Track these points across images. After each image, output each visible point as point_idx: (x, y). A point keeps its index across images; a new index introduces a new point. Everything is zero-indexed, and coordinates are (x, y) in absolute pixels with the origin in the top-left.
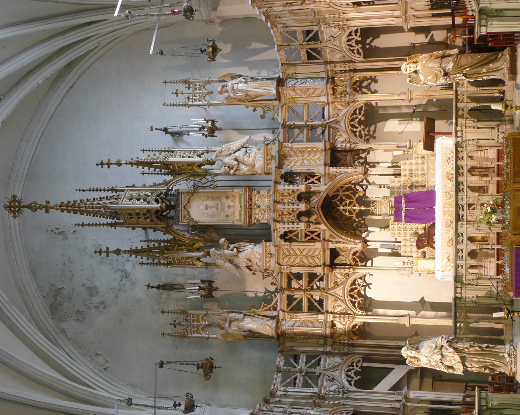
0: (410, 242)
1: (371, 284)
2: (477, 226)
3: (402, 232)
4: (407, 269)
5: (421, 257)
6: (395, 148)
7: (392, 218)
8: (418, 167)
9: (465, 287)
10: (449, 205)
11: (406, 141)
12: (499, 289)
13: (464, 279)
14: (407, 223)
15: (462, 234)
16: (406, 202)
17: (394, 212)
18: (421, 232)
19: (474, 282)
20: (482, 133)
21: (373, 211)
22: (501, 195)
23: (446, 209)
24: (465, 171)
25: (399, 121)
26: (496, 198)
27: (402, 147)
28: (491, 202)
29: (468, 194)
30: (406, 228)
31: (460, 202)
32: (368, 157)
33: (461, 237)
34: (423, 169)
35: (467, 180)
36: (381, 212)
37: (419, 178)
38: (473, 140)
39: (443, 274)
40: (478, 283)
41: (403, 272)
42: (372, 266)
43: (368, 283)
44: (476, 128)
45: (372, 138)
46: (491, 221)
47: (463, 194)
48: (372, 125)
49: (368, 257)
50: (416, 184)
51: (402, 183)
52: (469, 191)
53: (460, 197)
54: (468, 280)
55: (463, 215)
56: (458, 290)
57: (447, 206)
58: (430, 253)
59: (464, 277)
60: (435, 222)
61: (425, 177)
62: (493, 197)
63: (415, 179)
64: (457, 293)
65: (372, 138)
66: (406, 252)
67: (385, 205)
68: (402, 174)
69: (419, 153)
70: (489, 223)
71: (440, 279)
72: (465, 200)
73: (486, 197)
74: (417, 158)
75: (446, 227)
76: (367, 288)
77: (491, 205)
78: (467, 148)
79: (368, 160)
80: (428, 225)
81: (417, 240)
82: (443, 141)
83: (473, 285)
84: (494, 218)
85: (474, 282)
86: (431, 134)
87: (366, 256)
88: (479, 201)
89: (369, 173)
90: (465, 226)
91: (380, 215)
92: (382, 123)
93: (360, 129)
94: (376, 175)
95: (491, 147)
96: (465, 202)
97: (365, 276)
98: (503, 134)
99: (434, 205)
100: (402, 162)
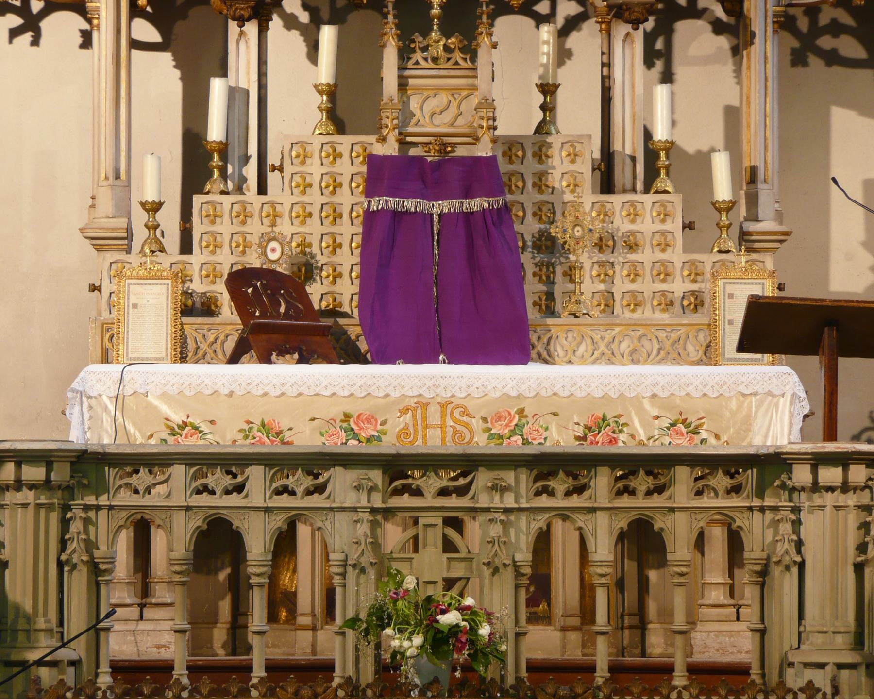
0: (266, 239)
1: (35, 42)
2: (365, 561)
3: (315, 198)
4: (122, 222)
6: (746, 164)
7: (390, 149)
8: (648, 278)
9: (49, 507)
10: (456, 432)
11: (779, 217)
12: (44, 672)
13: (90, 500)
14: (358, 222)
15: (320, 489)
16: (468, 216)
17: (420, 160)
18: (315, 291)
19: (76, 551)
20: (834, 586)
21: (425, 49)
22: (518, 679)
23: (434, 417)
24: (639, 502)
26: (504, 654)
27: (753, 200)
28: (484, 631)
29: (523, 521)
31: (483, 478)
32: (701, 26)
33: (308, 482)
34: (635, 302)
35: (593, 510)
36: (419, 89)
38: (799, 544)
39: (105, 399)
40: (74, 567)
41: (106, 205)
42: (136, 45)
43: (44, 24)
44: (859, 559)
45: (796, 44)
46: (389, 631)
47: (523, 490)
48: (868, 49)
49: (179, 27)
50: (559, 270)
51: (568, 197)
52: (540, 521)
53: (509, 477)
54: (87, 521)
55: (418, 492)
56: (34, 473)
57: (450, 423)
58: (211, 338)
59: (103, 500)
60: (365, 361)
61: (595, 312)
62: (511, 636)
63: (587, 266)
64: (18, 465)
65: (796, 44)
66: (214, 218)
67: (453, 109)
68: (616, 200)
69: (720, 283)
70: (380, 619)
71: (74, 385)
72: (497, 503)
73: (509, 603)
74: (696, 275)
75: (347, 416)
76: (15, 21)
77: (474, 630)
78: (757, 515)
79: (683, 28)
80: (354, 331)
81: (273, 272)
82: (784, 403)
83: (63, 544)
84: (406, 644)
85: (76, 551)
86: (829, 336)
87: (184, 17)
88: (487, 572)
89: (621, 29)
90: (364, 503)
91: (403, 86)
94: (607, 65)
95: (763, 632)
96: (484, 501)
98: (829, 690)
99: (453, 359)
100: (676, 200)
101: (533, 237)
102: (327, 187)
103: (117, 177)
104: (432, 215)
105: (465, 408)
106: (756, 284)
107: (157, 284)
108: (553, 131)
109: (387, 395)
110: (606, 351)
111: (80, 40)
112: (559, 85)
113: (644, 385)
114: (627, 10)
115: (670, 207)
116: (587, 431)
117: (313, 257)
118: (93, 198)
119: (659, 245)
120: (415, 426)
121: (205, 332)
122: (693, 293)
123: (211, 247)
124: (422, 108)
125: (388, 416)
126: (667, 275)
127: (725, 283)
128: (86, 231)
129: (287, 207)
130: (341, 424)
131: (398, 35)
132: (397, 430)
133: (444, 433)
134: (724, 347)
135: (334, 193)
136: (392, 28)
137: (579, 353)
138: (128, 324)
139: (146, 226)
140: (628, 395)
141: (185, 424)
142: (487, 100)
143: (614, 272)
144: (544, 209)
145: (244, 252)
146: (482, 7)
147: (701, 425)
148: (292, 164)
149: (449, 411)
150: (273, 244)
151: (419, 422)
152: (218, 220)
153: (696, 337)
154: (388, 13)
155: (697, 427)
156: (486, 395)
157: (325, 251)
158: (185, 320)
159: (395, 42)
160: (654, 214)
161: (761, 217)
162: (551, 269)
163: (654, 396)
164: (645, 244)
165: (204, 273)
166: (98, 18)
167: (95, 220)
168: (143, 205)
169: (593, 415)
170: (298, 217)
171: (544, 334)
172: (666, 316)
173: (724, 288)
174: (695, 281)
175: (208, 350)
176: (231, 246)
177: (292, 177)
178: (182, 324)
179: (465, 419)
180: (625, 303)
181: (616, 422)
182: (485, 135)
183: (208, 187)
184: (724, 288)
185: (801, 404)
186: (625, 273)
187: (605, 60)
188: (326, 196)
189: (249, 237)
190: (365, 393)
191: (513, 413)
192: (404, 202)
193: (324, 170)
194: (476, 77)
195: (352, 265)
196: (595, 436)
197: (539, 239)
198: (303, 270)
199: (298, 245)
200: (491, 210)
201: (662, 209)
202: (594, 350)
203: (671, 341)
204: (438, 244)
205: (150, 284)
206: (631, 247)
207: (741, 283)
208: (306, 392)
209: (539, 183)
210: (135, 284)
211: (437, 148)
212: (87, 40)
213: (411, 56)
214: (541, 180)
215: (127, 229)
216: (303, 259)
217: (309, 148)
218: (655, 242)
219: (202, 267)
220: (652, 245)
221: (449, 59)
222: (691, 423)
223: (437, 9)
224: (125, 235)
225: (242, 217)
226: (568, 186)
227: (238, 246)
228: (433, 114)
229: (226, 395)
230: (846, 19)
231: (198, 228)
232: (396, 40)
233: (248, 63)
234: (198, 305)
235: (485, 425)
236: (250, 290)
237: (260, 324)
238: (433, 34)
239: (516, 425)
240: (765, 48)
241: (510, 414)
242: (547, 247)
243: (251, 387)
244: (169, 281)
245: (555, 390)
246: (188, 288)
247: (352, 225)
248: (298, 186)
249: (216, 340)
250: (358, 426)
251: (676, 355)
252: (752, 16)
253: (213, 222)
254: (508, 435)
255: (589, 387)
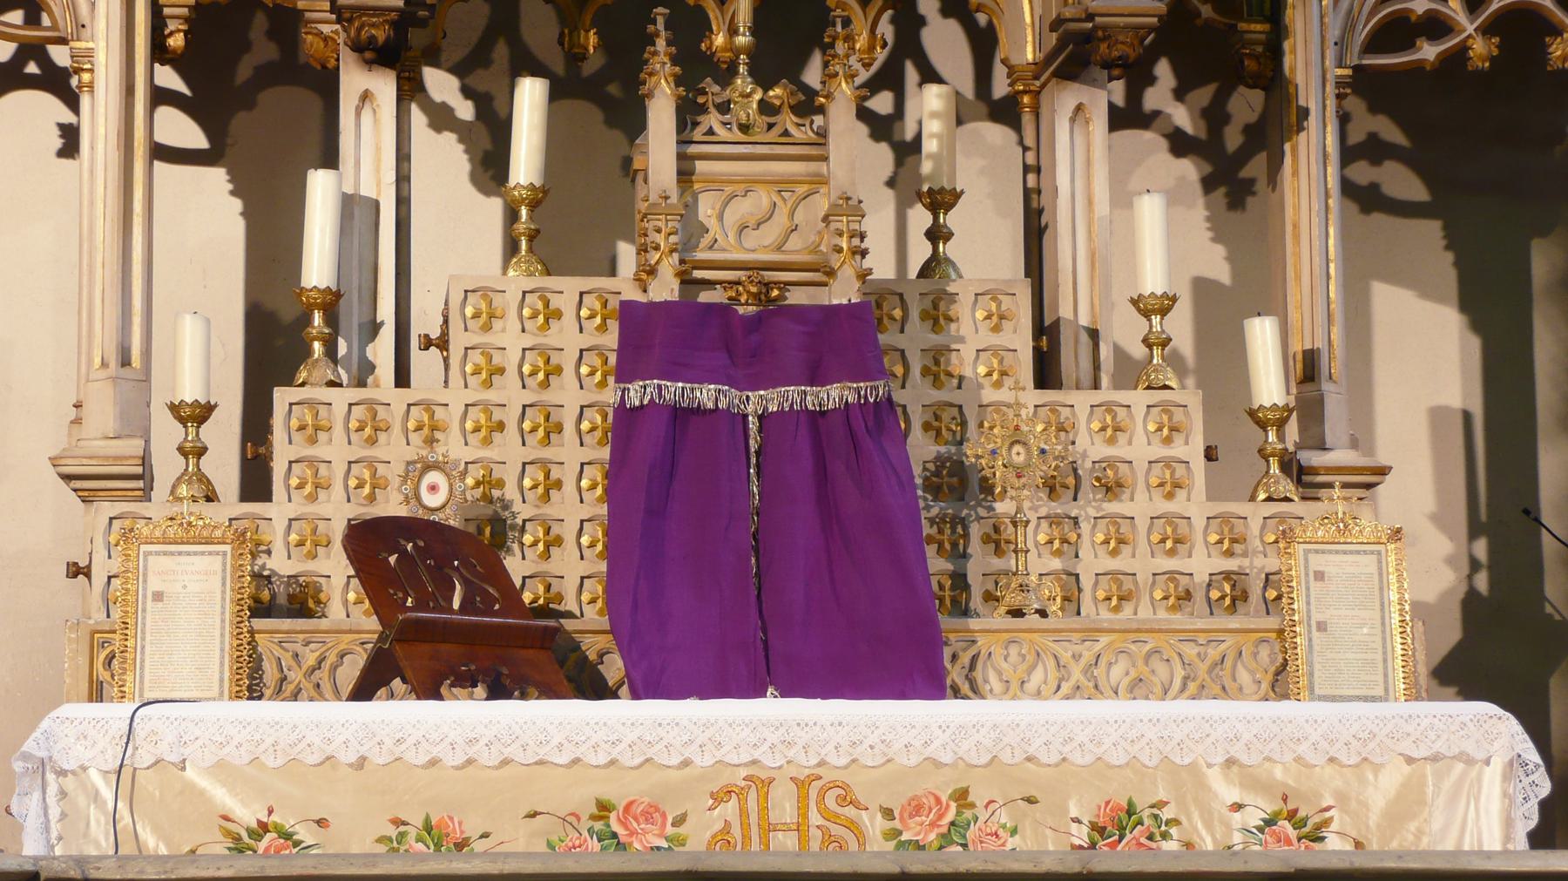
3: (511, 394)
4: (134, 446)
5: (257, 576)
7: (665, 289)
10: (828, 838)
21: (724, 108)
23: (784, 808)
25: (1467, 417)
27: (1309, 408)
30: (553, 429)
36: (716, 182)
37: (1040, 563)
39: (95, 776)
41: (103, 414)
49: (240, 123)
50: (975, 530)
51: (989, 395)
57: (815, 819)
58: (310, 659)
66: (314, 431)
67: (781, 220)
68: (1079, 402)
71: (29, 746)
74: (1233, 542)
75: (604, 808)
80: (592, 646)
82: (1492, 776)
87: (250, 105)
91: (685, 175)
92: (1444, 266)
93: (1468, 26)
97: (60, 84)
101: (925, 469)
102: (533, 374)
103: (125, 362)
104: (745, 416)
105: (845, 787)
106: (1365, 552)
107: (203, 553)
108: (953, 276)
109: (686, 763)
110: (1084, 681)
111: (58, 143)
112: (962, 192)
113: (1210, 740)
114: (1104, 39)
115: (1178, 415)
116: (1096, 836)
117: (506, 506)
118: (78, 406)
119: (1161, 485)
120: (746, 827)
121: (298, 647)
122: (1227, 575)
123: (308, 488)
124: (721, 217)
125: (688, 806)
126: (1177, 541)
127: (1307, 552)
128: (63, 462)
129: (457, 410)
130: (591, 823)
131: (675, 76)
132: (708, 835)
133: (803, 840)
134: (1311, 674)
135: (545, 384)
136: (664, 63)
137: (1031, 686)
138: (143, 632)
139: (181, 449)
140: (1178, 761)
141: (264, 827)
142: (848, 199)
143: (1079, 536)
144: (946, 416)
145: (372, 498)
146: (834, 25)
147: (1327, 823)
148: (466, 330)
149: (813, 794)
150: (433, 477)
151: (754, 818)
152: (322, 436)
153: (1255, 655)
154: (657, 34)
155: (1318, 827)
156: (889, 761)
157: (529, 495)
158: (259, 623)
159: (670, 88)
160: (1152, 427)
161: (1329, 442)
162: (960, 530)
163: (1230, 762)
164: (1134, 485)
165: (294, 537)
166: (91, 71)
167: (82, 443)
168: (175, 409)
169: (1107, 803)
170: (477, 430)
171: (965, 650)
172: (1178, 616)
173: (1306, 560)
174: (1229, 553)
175: (305, 684)
176: (346, 486)
177: (466, 355)
178: (252, 632)
179: (850, 811)
180: (1101, 594)
181: (1156, 817)
182: (845, 266)
183: (302, 375)
184: (1306, 560)
185: (1532, 778)
186: (1100, 537)
187: (1031, 158)
188: (533, 390)
189: (381, 469)
190: (641, 759)
191: (944, 799)
192: (692, 390)
193: (528, 341)
194: (825, 159)
195: (582, 522)
196: (1113, 846)
197: (937, 473)
198: (488, 531)
199: (478, 484)
200: (863, 406)
201: (1165, 418)
202: (1061, 680)
203: (1208, 662)
204: (758, 474)
205: (188, 554)
206: (1108, 489)
207: (1337, 552)
208: (519, 757)
209: (934, 368)
210: (158, 553)
211: (754, 289)
212: (70, 141)
213: (699, 119)
214: (937, 363)
215: (143, 458)
216: (488, 511)
217: (497, 300)
218: (1154, 481)
219: (290, 526)
220: (1148, 486)
221: (771, 126)
222: (1307, 818)
223: (744, 35)
224: (139, 470)
225: (368, 430)
226: (989, 374)
227: (360, 486)
228: (743, 228)
229: (351, 765)
230: (1391, 132)
231: (283, 450)
232: (673, 85)
233: (378, 149)
234: (282, 600)
235: (891, 824)
236: (392, 559)
237: (418, 621)
238: (739, 81)
239: (952, 824)
240: (1325, 138)
241: (938, 801)
242: (951, 488)
243: (403, 747)
244: (227, 548)
245: (1031, 750)
246: (263, 567)
247: (582, 445)
248: (476, 372)
249: (320, 663)
250: (626, 828)
251: (1217, 690)
252: (1300, 79)
253: (313, 441)
254: (936, 845)
255: (1100, 744)
